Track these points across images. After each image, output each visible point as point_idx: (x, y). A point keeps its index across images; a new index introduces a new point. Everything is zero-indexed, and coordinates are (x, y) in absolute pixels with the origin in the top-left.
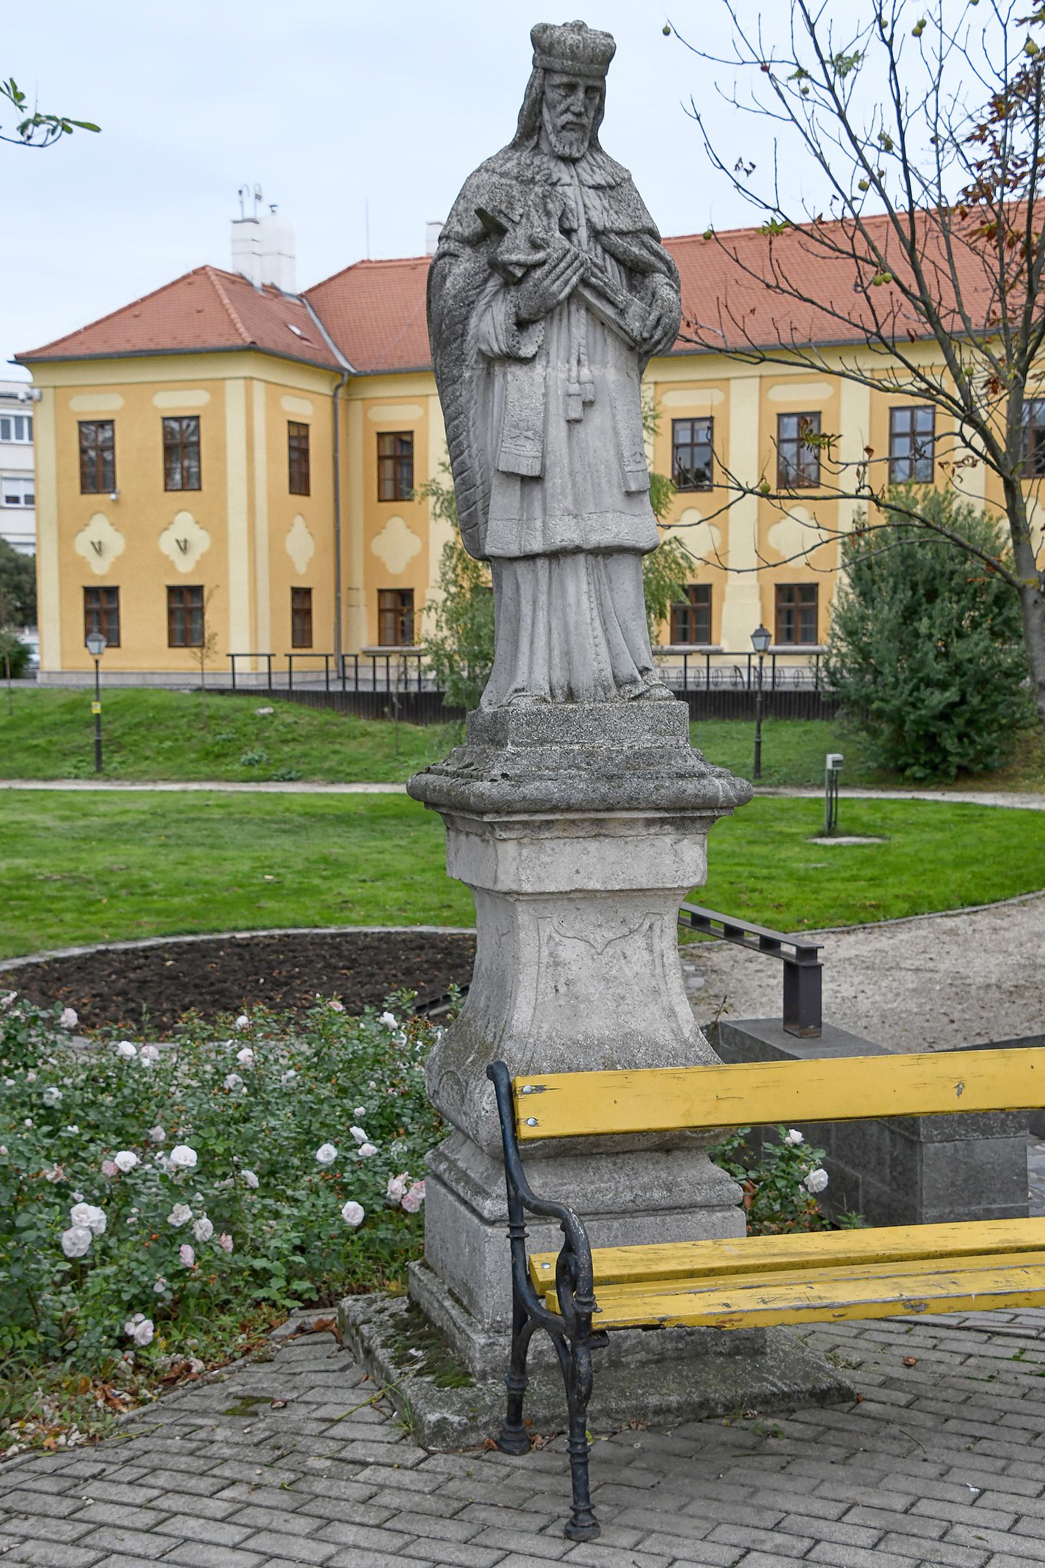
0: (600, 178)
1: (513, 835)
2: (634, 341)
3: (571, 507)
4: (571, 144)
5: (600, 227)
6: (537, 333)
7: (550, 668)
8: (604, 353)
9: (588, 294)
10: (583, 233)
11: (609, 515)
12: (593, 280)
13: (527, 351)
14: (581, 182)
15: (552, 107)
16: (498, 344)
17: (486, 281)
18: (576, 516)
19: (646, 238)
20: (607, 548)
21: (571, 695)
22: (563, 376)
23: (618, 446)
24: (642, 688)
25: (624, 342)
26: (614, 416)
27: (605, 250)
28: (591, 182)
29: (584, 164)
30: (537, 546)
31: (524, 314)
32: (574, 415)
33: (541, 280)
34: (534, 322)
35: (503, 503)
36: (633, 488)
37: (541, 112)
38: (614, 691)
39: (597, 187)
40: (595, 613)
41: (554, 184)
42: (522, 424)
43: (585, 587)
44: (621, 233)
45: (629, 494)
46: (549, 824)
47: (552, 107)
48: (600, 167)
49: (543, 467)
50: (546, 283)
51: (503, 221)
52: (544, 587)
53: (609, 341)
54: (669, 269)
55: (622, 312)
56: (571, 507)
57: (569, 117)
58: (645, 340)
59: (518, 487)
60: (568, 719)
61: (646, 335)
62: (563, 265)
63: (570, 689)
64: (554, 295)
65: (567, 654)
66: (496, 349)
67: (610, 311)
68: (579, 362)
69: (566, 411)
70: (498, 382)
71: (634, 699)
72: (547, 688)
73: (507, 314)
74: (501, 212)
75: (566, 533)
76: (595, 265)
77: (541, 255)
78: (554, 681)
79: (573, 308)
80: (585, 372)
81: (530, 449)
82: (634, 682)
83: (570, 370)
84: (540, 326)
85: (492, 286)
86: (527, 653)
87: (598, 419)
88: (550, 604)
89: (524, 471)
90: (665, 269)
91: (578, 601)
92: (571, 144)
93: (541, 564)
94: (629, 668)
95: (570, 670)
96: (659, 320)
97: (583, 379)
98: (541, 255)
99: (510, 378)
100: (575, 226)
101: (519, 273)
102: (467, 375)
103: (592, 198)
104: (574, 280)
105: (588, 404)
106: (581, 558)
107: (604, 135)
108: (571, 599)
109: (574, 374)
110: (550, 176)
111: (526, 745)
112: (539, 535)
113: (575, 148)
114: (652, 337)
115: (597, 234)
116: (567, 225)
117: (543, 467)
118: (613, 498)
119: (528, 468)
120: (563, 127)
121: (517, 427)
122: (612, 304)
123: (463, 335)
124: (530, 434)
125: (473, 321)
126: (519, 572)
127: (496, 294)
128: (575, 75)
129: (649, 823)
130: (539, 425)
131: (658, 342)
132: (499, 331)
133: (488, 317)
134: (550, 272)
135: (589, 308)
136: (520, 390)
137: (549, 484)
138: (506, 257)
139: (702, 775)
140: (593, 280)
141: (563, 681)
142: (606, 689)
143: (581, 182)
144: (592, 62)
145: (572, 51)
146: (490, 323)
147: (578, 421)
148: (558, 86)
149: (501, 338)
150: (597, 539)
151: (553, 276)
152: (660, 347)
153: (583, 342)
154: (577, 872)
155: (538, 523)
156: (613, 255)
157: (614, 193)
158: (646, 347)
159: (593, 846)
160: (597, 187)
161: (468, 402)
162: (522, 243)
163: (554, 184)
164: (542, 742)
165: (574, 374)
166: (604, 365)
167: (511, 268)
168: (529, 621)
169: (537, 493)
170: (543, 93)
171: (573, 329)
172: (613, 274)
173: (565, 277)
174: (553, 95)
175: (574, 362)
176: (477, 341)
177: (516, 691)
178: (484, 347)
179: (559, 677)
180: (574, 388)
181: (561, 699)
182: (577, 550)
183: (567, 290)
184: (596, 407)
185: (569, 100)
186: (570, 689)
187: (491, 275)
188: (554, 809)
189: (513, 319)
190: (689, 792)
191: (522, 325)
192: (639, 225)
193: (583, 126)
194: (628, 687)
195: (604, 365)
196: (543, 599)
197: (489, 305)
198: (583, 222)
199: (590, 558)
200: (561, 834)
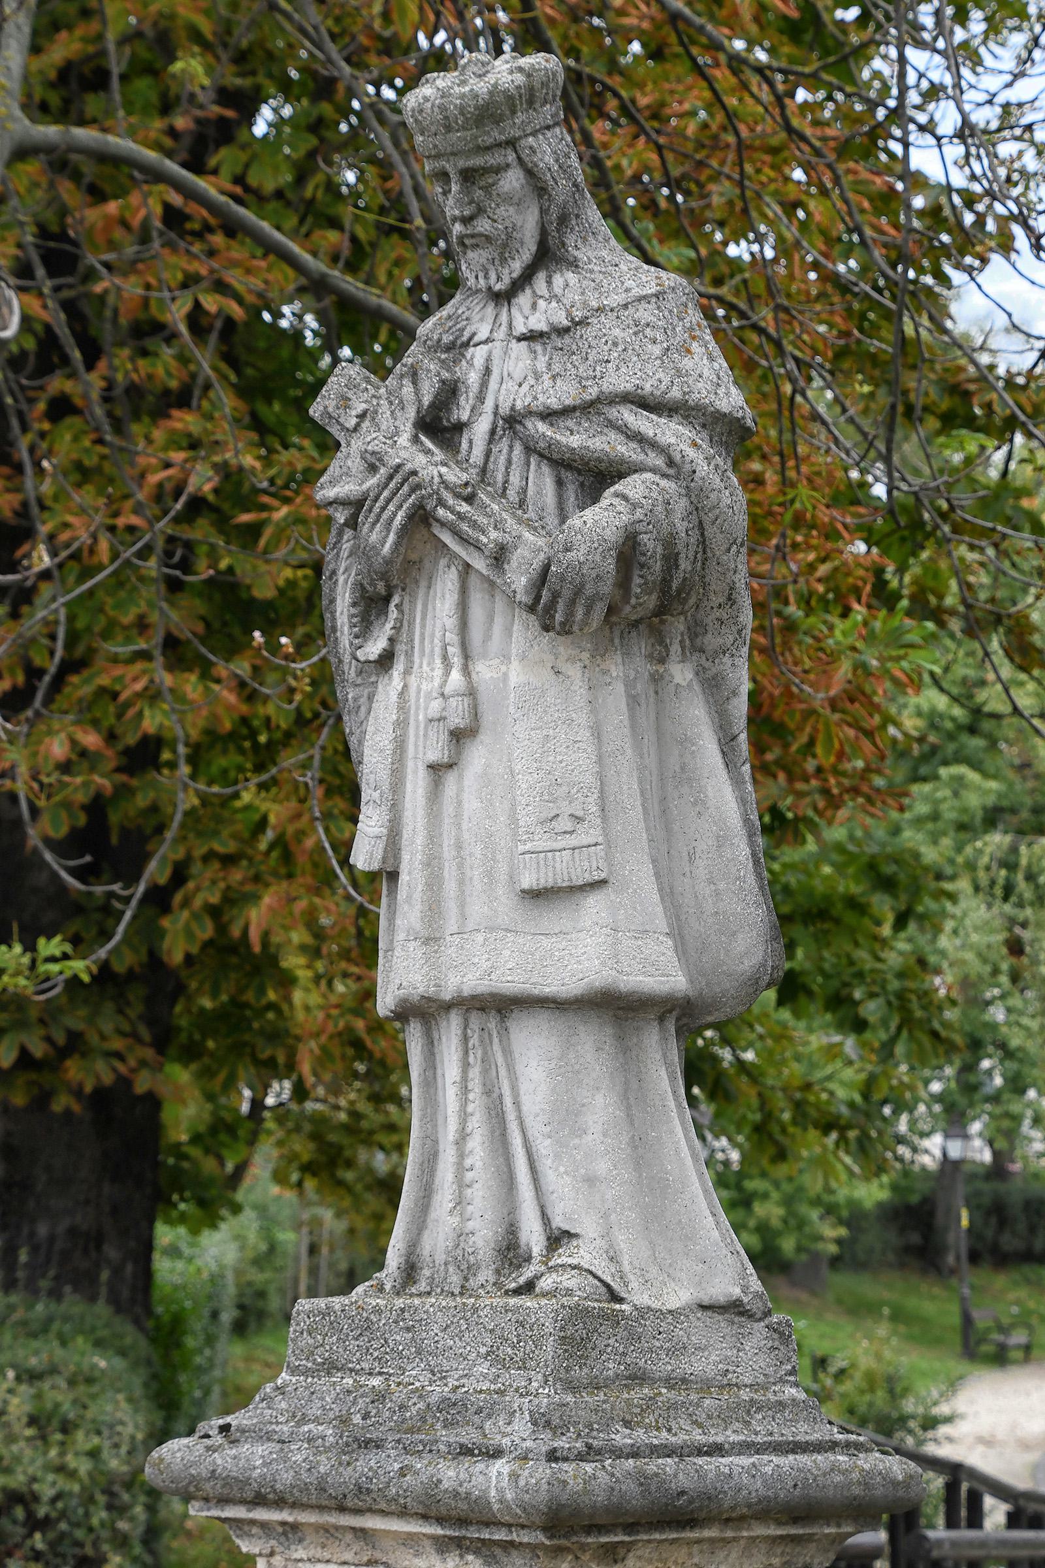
3: (418, 926)
8: (508, 631)
10: (482, 427)
11: (480, 938)
12: (441, 512)
18: (427, 941)
19: (613, 413)
20: (474, 997)
27: (529, 450)
29: (523, 299)
32: (433, 756)
36: (528, 881)
38: (486, 1275)
39: (531, 337)
41: (466, 345)
44: (549, 415)
46: (291, 1530)
51: (334, 430)
54: (671, 463)
60: (368, 1327)
62: (386, 494)
71: (517, 1292)
79: (443, 562)
87: (477, 757)
90: (660, 462)
96: (546, 568)
97: (448, 690)
100: (463, 413)
103: (519, 359)
105: (460, 737)
109: (437, 682)
111: (306, 1372)
113: (493, 276)
114: (538, 598)
122: (478, 548)
140: (441, 512)
144: (448, 129)
153: (451, 622)
156: (541, 455)
157: (567, 340)
162: (355, 464)
164: (331, 1367)
166: (506, 658)
173: (385, 516)
175: (438, 661)
184: (484, 737)
188: (259, 1500)
192: (593, 392)
193: (488, 238)
195: (506, 658)
199: (475, 1019)
200: (319, 1553)
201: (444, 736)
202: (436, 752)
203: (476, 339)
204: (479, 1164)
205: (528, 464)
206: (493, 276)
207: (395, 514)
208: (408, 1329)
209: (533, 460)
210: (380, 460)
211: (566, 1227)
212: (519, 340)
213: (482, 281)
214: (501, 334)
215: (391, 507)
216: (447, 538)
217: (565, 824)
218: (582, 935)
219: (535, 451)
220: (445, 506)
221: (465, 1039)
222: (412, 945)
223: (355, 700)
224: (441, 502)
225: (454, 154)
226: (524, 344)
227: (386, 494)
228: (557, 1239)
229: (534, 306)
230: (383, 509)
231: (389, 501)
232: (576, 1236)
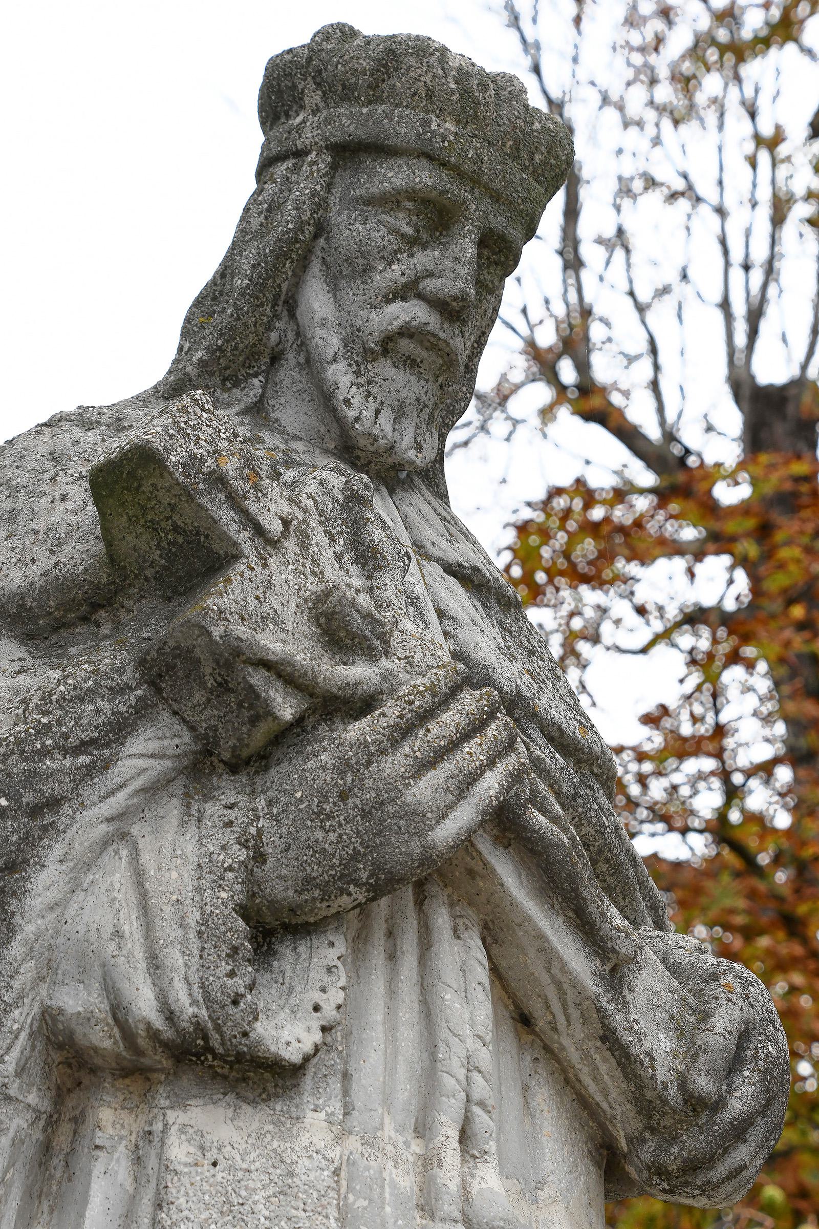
2: (647, 1103)
4: (400, 414)
13: (286, 1033)
17: (119, 730)
25: (584, 1109)
31: (280, 884)
33: (373, 753)
47: (348, 271)
50: (394, 764)
57: (411, 312)
64: (419, 820)
70: (105, 1184)
74: (218, 480)
77: (360, 672)
84: (331, 951)
98: (360, 672)
99: (179, 1151)
104: (491, 784)
120: (387, 344)
125: (45, 883)
127: (153, 791)
128: (459, 173)
132: (167, 930)
133: (115, 875)
135: (497, 932)
145: (466, 93)
148: (389, 201)
149: (175, 958)
151: (415, 746)
158: (693, 1142)
170: (321, 229)
176: (49, 972)
178: (77, 1000)
197: (119, 833)
210: (384, 638)
215: (474, 751)
220: (544, 811)
225: (496, 197)
231: (466, 736)
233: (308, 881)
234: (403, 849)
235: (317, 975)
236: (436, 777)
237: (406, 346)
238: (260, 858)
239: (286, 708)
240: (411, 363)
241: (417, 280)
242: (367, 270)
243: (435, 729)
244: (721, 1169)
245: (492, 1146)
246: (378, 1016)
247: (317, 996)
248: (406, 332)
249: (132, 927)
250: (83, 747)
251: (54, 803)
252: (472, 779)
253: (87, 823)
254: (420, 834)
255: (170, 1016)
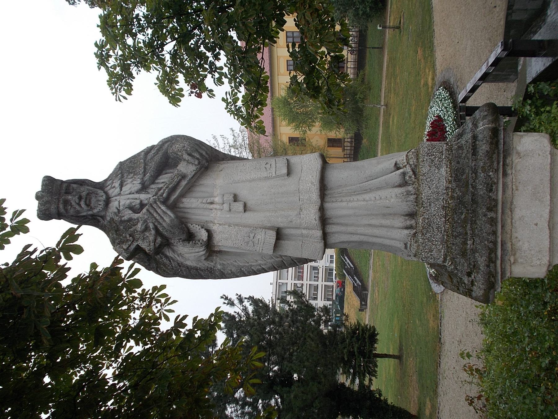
0: (117, 184)
1: (508, 267)
2: (201, 169)
4: (99, 201)
5: (139, 186)
6: (195, 228)
7: (393, 227)
9: (173, 197)
11: (301, 187)
12: (165, 195)
13: (204, 235)
14: (119, 194)
15: (78, 212)
16: (201, 251)
17: (167, 257)
19: (149, 157)
20: (321, 190)
21: (412, 215)
22: (219, 212)
23: (260, 179)
24: (408, 169)
26: (243, 181)
27: (153, 183)
28: (118, 189)
29: (110, 192)
30: (319, 233)
31: (184, 237)
32: (241, 208)
34: (188, 229)
35: (291, 249)
36: (285, 171)
37: (84, 216)
38: (410, 188)
39: (121, 186)
40: (360, 197)
41: (119, 210)
42: (246, 239)
43: (344, 204)
45: (289, 174)
48: (113, 183)
49: (270, 228)
50: (164, 224)
52: (343, 229)
53: (201, 182)
55: (184, 177)
56: (296, 212)
57: (82, 203)
58: (199, 163)
59: (283, 242)
61: (196, 163)
62: (155, 215)
63: (407, 215)
65: (384, 215)
66: (204, 252)
67: (184, 183)
68: (212, 203)
69: (239, 212)
72: (406, 232)
73: (184, 246)
75: (311, 215)
76: (156, 194)
78: (401, 225)
79: (181, 205)
80: (217, 199)
81: (260, 235)
82: (404, 174)
83: (216, 209)
85: (170, 254)
86: (382, 239)
87: (244, 193)
88: (352, 225)
89: (273, 241)
91: (352, 208)
92: (99, 201)
93: (330, 229)
94: (396, 176)
95: (395, 214)
96: (189, 155)
97: (221, 201)
98: (151, 226)
100: (138, 201)
101: (159, 240)
102: (219, 267)
104: (163, 208)
105: (236, 198)
106: (327, 205)
107: (98, 177)
108: (351, 212)
109: (218, 207)
110: (115, 213)
112: (311, 232)
114: (197, 159)
115: (144, 188)
116: (138, 206)
117: (270, 228)
118: (291, 184)
119: (271, 236)
121: (248, 243)
123: (197, 269)
124: (252, 236)
125: (189, 263)
126: (333, 241)
127: (174, 251)
129: (505, 174)
130: (247, 230)
131: (201, 155)
132: (193, 251)
134: (159, 222)
136: (227, 239)
137: (281, 225)
138: (152, 247)
139: (475, 137)
141: (402, 219)
142: (408, 193)
143: (119, 194)
146: (189, 255)
147: (245, 205)
149: (197, 250)
150: (315, 196)
151: (161, 221)
152: (204, 153)
153: (200, 200)
154: (536, 225)
155: (305, 232)
159: (518, 213)
160: (121, 186)
161: (234, 266)
163: (119, 210)
165: (218, 207)
167: (157, 245)
168: (363, 237)
169: (287, 231)
171: (193, 206)
172: (165, 179)
173: (161, 213)
174: (72, 212)
175: (212, 206)
176: (200, 261)
177: (406, 248)
178: (203, 258)
179: (399, 222)
180: (226, 206)
181: (413, 222)
182: (322, 209)
183: (169, 212)
184: (238, 192)
185: (73, 203)
186: (407, 215)
187: (163, 254)
189: (186, 243)
190: (488, 149)
191: (190, 237)
193: (88, 194)
194: (407, 178)
196: (350, 229)
197: (180, 255)
198: (137, 196)
199: (327, 199)
201: (236, 204)
202: (239, 206)
203: (118, 206)
204: (374, 195)
205: (158, 183)
206: (101, 198)
207: (162, 210)
208: (430, 205)
209: (156, 181)
211: (394, 164)
212: (121, 190)
213: (100, 203)
214: (118, 197)
215: (159, 211)
216: (173, 197)
217: (268, 166)
218: (303, 161)
219: (154, 181)
220: (163, 194)
221: (333, 202)
222: (302, 216)
223: (220, 265)
224: (162, 195)
226: (123, 188)
227: (155, 215)
228: (397, 167)
229: (114, 187)
230: (159, 215)
232: (396, 162)
233: (183, 233)
234: (176, 222)
235: (194, 228)
236: (165, 218)
237: (88, 202)
238: (181, 239)
239: (159, 240)
240: (90, 200)
241: (77, 204)
242: (78, 211)
243: (157, 218)
244: (207, 156)
245: (212, 199)
246: (198, 217)
247: (198, 229)
248: (86, 204)
249: (194, 254)
250: (170, 262)
251: (178, 264)
252: (163, 211)
253: (180, 259)
254: (173, 220)
255: (204, 250)
